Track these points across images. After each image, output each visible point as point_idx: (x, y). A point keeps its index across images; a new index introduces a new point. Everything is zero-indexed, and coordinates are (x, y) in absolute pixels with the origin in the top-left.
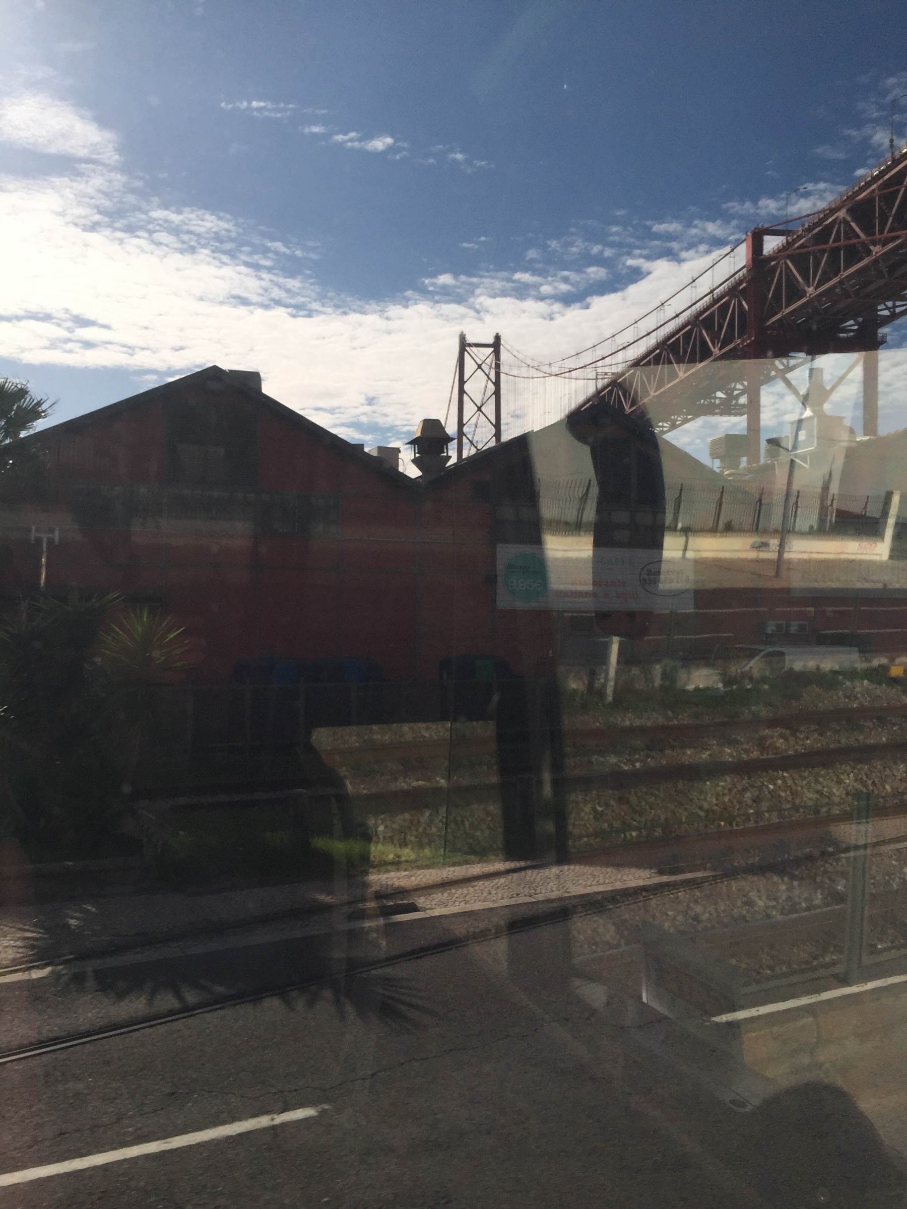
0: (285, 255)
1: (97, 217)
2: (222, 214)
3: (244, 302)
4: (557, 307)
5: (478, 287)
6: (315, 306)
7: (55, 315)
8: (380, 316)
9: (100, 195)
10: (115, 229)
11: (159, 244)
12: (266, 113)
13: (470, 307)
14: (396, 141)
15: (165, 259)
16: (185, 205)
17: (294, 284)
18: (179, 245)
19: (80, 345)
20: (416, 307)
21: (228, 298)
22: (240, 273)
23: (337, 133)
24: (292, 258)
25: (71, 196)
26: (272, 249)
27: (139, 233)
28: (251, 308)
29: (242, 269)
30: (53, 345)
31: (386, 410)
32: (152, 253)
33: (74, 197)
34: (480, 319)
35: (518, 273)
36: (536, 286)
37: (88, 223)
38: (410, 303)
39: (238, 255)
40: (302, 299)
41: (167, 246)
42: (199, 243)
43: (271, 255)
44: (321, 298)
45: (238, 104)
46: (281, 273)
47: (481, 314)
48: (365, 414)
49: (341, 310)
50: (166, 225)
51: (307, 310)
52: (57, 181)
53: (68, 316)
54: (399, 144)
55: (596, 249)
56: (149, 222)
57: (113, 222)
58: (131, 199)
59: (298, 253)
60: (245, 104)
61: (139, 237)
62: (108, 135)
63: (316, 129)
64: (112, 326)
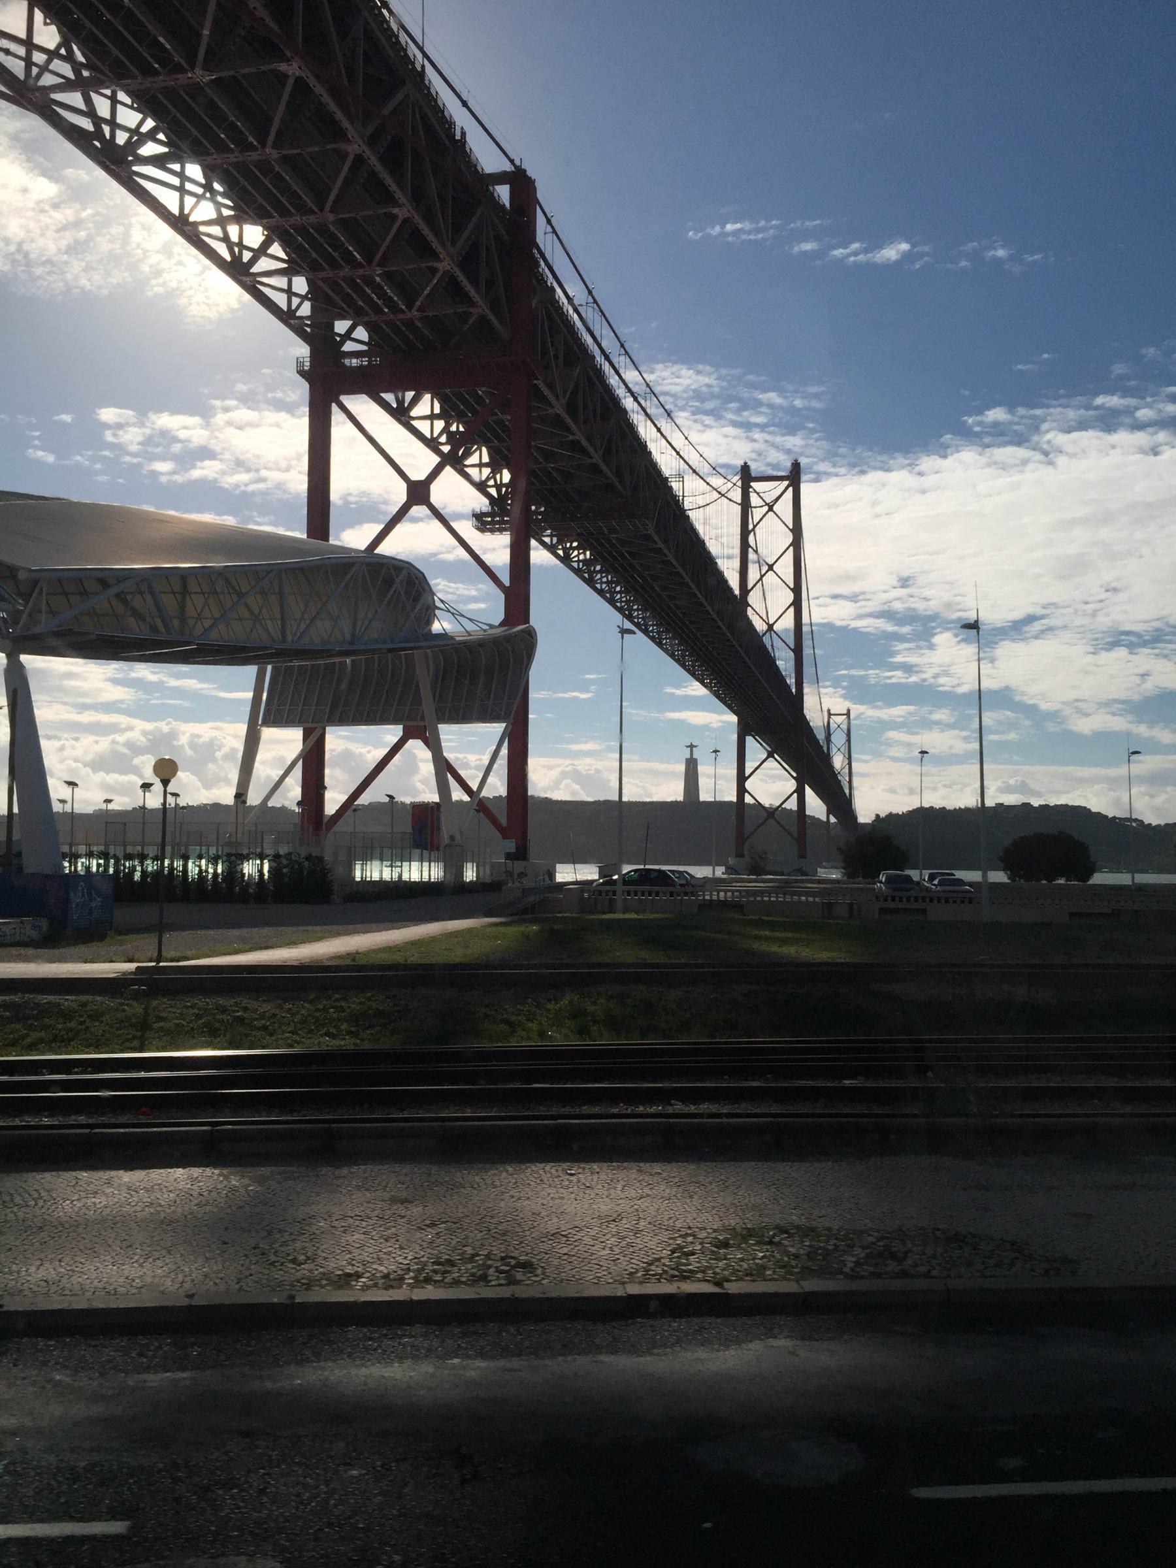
0: (781, 408)
2: (700, 367)
4: (1162, 436)
5: (1044, 420)
6: (823, 467)
8: (910, 472)
12: (744, 237)
13: (1034, 449)
14: (913, 246)
16: (658, 362)
20: (956, 456)
22: (727, 436)
23: (836, 247)
24: (793, 411)
26: (765, 401)
29: (731, 430)
31: (927, 593)
34: (1051, 463)
35: (1101, 396)
36: (1130, 411)
38: (949, 451)
39: (724, 413)
42: (676, 406)
43: (763, 409)
45: (709, 230)
46: (777, 430)
47: (1051, 456)
49: (857, 469)
51: (814, 473)
54: (918, 249)
59: (798, 403)
60: (718, 229)
63: (808, 246)
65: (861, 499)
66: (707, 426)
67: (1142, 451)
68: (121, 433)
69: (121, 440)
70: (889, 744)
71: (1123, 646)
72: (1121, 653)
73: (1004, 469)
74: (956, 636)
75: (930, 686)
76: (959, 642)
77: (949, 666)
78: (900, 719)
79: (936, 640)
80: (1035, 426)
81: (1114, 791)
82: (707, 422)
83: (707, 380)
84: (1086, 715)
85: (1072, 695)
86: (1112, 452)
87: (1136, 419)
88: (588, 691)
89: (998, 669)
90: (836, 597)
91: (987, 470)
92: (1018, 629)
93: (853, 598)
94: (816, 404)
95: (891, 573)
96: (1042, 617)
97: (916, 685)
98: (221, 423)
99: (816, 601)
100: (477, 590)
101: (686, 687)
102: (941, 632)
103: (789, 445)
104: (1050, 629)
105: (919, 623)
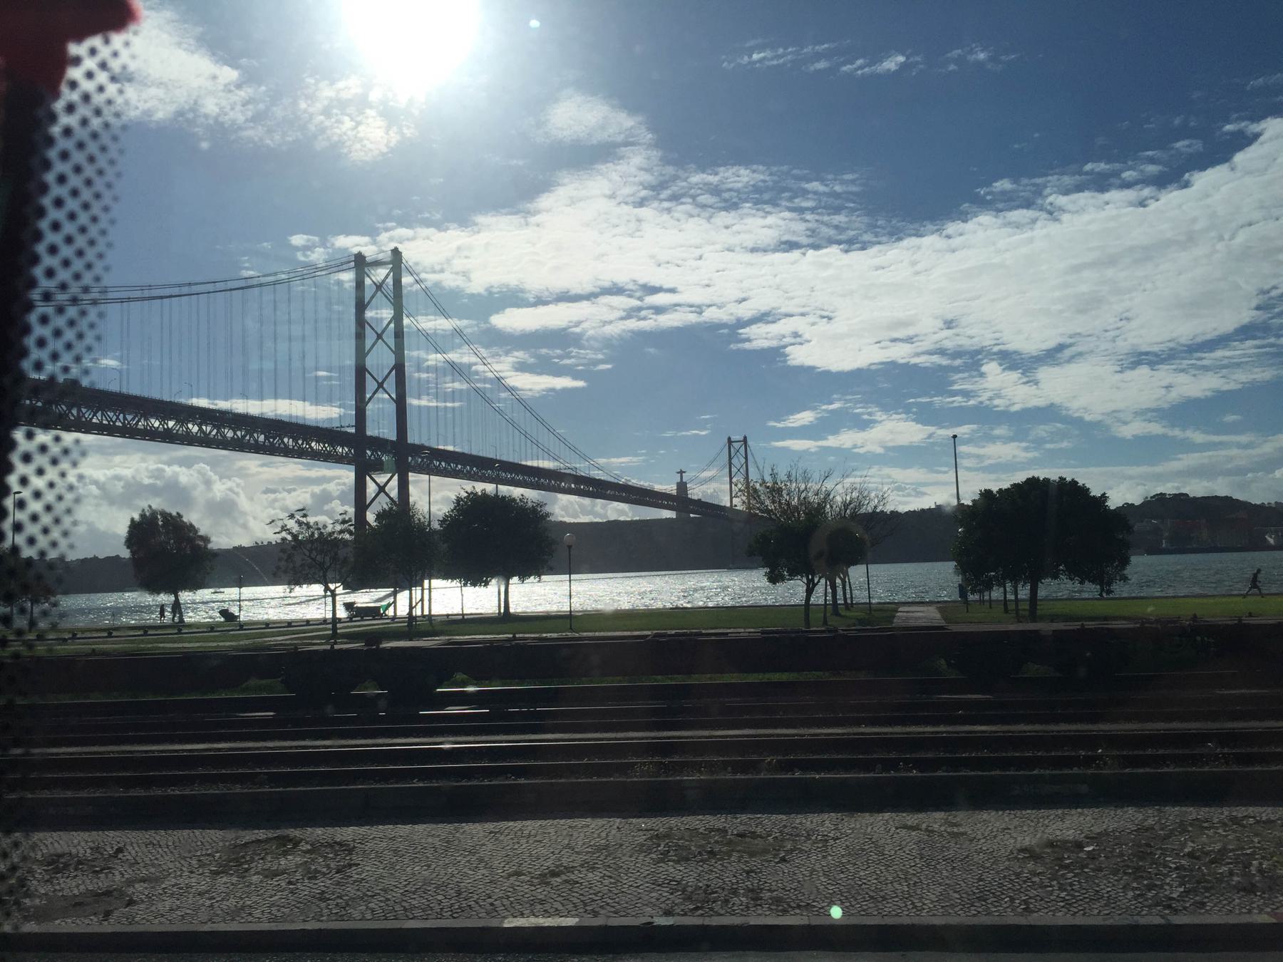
0: (824, 194)
1: (644, 193)
2: (755, 167)
3: (790, 246)
4: (1147, 192)
5: (1045, 187)
6: (867, 237)
7: (626, 287)
8: (940, 236)
9: (642, 172)
10: (661, 200)
11: (704, 206)
13: (1041, 210)
16: (720, 166)
17: (840, 219)
19: (651, 311)
20: (975, 220)
22: (785, 220)
24: (836, 195)
25: (618, 179)
27: (683, 200)
28: (803, 250)
29: (787, 214)
30: (631, 313)
31: (970, 332)
32: (699, 216)
33: (620, 179)
34: (1056, 220)
37: (638, 200)
38: (969, 216)
39: (779, 202)
40: (852, 233)
41: (711, 207)
42: (740, 199)
44: (872, 227)
46: (824, 211)
47: (1055, 214)
48: (946, 338)
50: (706, 188)
52: (602, 167)
53: (636, 287)
55: (1177, 121)
57: (659, 194)
58: (670, 170)
59: (838, 188)
61: (682, 203)
62: (640, 118)
64: (679, 290)
65: (902, 262)
67: (1131, 204)
68: (309, 253)
69: (311, 258)
71: (1145, 364)
72: (1144, 370)
73: (1018, 228)
74: (1001, 365)
75: (987, 406)
76: (1004, 369)
78: (966, 436)
79: (984, 369)
80: (1039, 192)
81: (1145, 485)
82: (767, 210)
83: (762, 177)
84: (1126, 423)
86: (1107, 207)
87: (1124, 180)
88: (704, 429)
90: (894, 340)
92: (1053, 356)
93: (909, 340)
95: (936, 318)
96: (1071, 345)
97: (975, 407)
98: (386, 240)
100: (603, 354)
101: (784, 421)
102: (987, 363)
103: (835, 222)
104: (1080, 354)
105: (967, 357)
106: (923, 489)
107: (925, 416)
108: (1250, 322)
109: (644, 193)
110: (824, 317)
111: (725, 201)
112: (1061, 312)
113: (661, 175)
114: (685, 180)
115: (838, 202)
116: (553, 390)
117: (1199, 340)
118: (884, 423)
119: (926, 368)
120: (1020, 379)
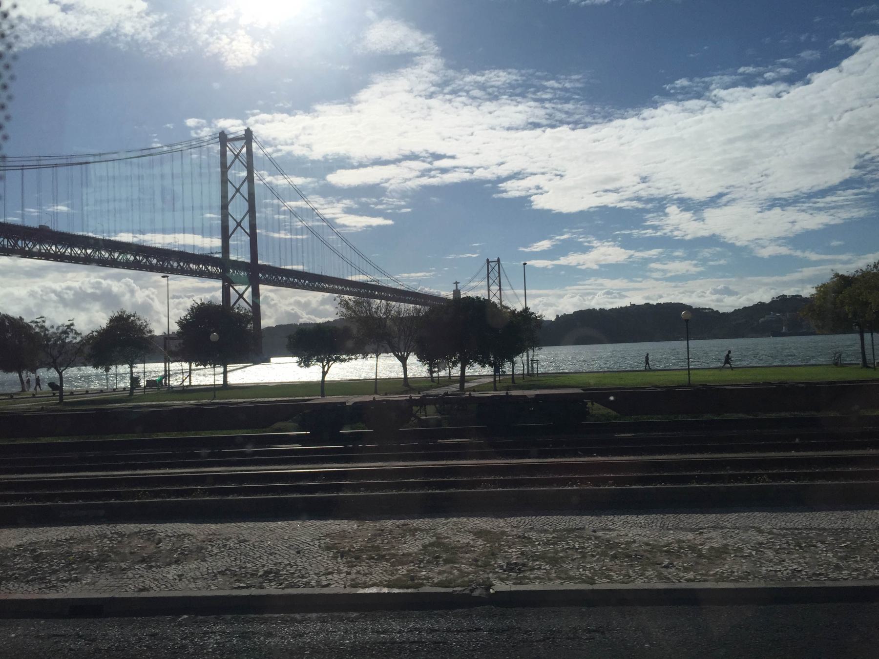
0: (558, 89)
1: (433, 89)
2: (510, 70)
3: (536, 126)
4: (782, 87)
6: (588, 119)
7: (420, 155)
8: (638, 118)
10: (445, 94)
11: (474, 98)
15: (480, 108)
16: (485, 70)
17: (569, 106)
18: (486, 97)
19: (439, 172)
20: (662, 107)
21: (527, 126)
22: (531, 107)
24: (566, 90)
25: (415, 79)
27: (460, 94)
28: (543, 129)
29: (532, 104)
30: (424, 173)
31: (659, 185)
32: (471, 105)
34: (719, 107)
37: (427, 94)
38: (658, 105)
39: (527, 95)
42: (500, 93)
43: (548, 90)
44: (591, 113)
46: (558, 101)
47: (718, 103)
48: (642, 189)
49: (607, 119)
52: (403, 71)
53: (428, 155)
55: (803, 38)
56: (465, 85)
57: (443, 90)
58: (451, 73)
59: (568, 85)
61: (461, 96)
62: (429, 36)
65: (612, 136)
66: (519, 102)
67: (771, 96)
68: (199, 131)
70: (652, 271)
71: (779, 206)
72: (777, 210)
73: (692, 112)
74: (679, 207)
75: (669, 236)
76: (681, 211)
77: (678, 225)
78: (654, 257)
79: (667, 210)
80: (707, 88)
81: (775, 289)
83: (514, 77)
84: (764, 247)
85: (755, 236)
86: (754, 97)
87: (765, 79)
88: (475, 253)
89: (707, 224)
90: (606, 191)
91: (682, 114)
92: (714, 201)
93: (616, 191)
94: (578, 85)
95: (635, 175)
96: (727, 194)
98: (253, 122)
99: (595, 194)
100: (405, 201)
101: (530, 247)
104: (734, 200)
105: (657, 202)
106: (624, 293)
107: (627, 243)
108: (850, 177)
109: (433, 89)
110: (557, 175)
111: (490, 94)
112: (720, 171)
113: (445, 76)
114: (462, 80)
115: (568, 95)
116: (370, 226)
117: (816, 189)
118: (598, 248)
119: (628, 210)
120: (692, 217)
